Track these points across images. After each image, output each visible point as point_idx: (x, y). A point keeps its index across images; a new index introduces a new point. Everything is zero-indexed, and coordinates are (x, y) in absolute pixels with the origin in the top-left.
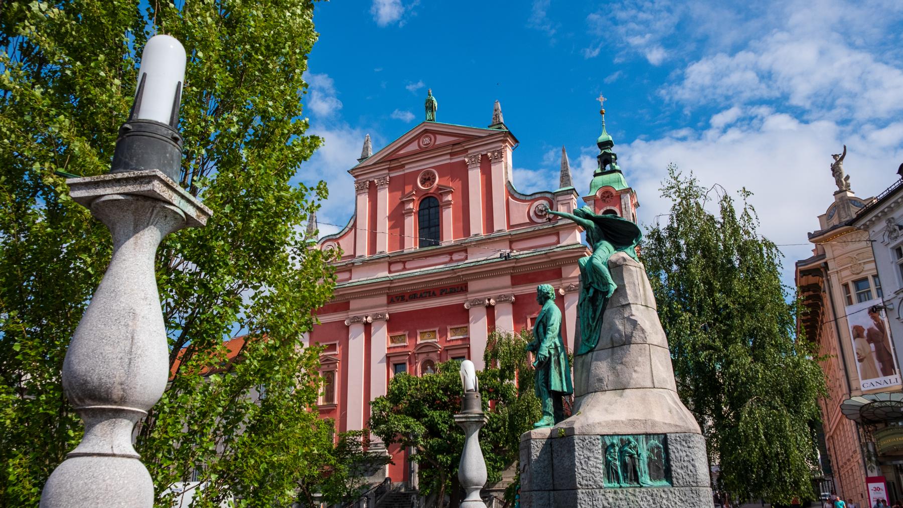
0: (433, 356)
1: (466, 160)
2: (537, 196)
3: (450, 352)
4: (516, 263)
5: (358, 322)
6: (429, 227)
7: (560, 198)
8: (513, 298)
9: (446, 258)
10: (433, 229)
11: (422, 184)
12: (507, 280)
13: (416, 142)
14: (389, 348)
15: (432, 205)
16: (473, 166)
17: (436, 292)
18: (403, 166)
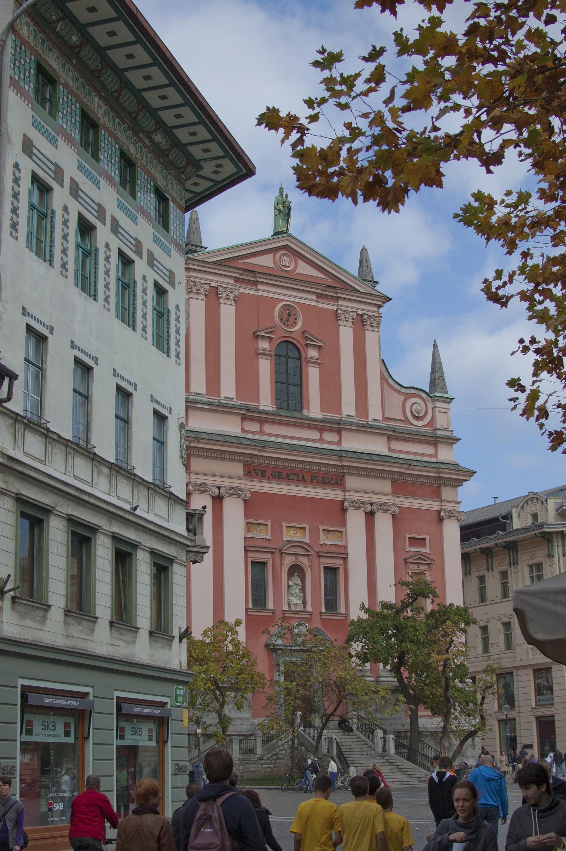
0: (304, 562)
1: (340, 311)
2: (413, 391)
3: (323, 560)
4: (406, 469)
5: (205, 491)
6: (288, 384)
7: (438, 404)
8: (397, 510)
9: (315, 435)
10: (291, 388)
11: (281, 320)
12: (387, 486)
13: (270, 256)
14: (246, 538)
15: (290, 354)
16: (345, 323)
17: (306, 477)
18: (256, 283)
